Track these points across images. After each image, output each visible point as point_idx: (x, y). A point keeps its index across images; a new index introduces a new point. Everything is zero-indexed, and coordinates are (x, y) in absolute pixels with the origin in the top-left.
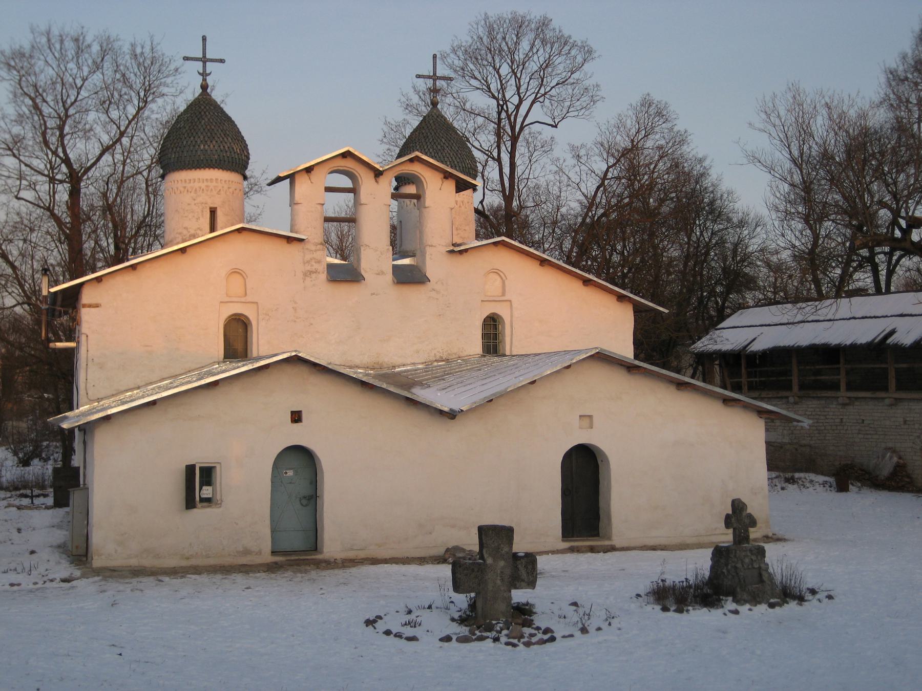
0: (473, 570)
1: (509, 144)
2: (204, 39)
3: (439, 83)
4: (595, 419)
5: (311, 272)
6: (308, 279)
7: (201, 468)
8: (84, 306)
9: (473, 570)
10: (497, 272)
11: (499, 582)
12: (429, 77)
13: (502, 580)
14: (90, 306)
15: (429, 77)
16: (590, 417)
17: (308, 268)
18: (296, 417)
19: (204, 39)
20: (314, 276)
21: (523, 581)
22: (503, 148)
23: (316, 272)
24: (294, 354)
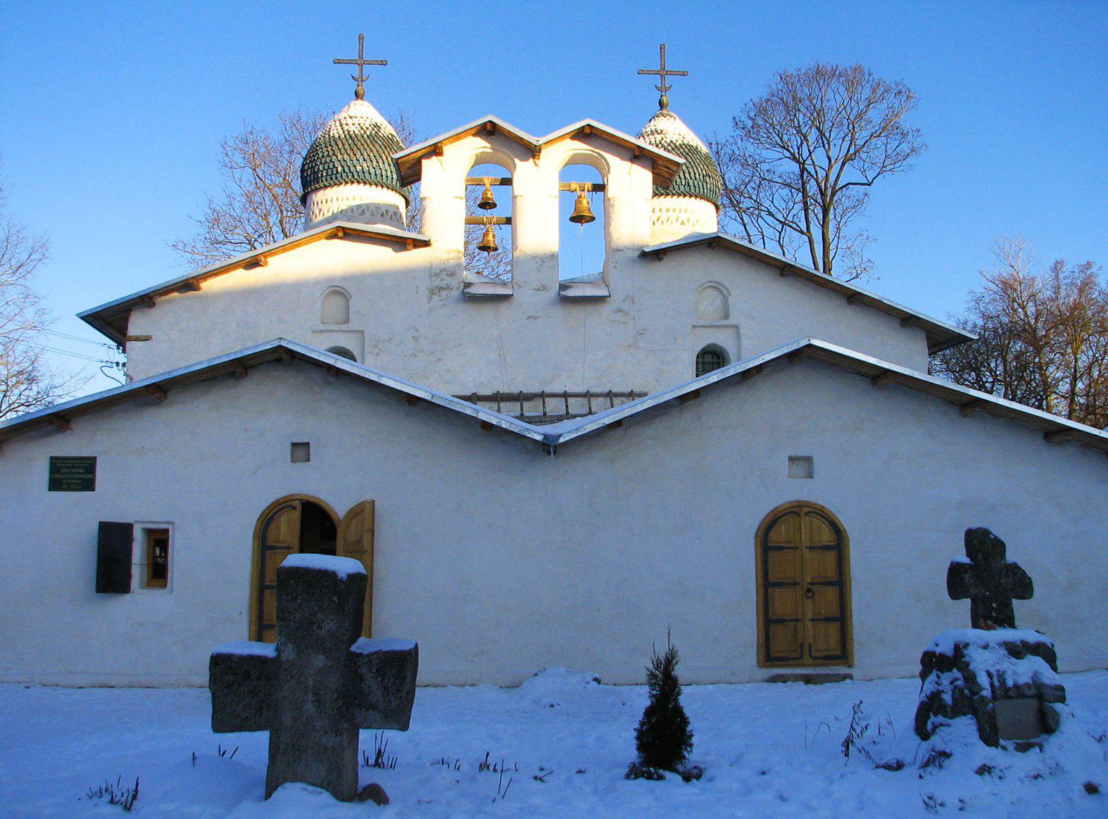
0: (247, 675)
1: (819, 210)
2: (361, 38)
3: (669, 80)
4: (816, 462)
5: (441, 289)
6: (436, 298)
7: (149, 532)
8: (131, 339)
9: (247, 675)
10: (717, 287)
11: (310, 708)
12: (656, 73)
13: (319, 702)
14: (137, 339)
15: (656, 73)
16: (808, 460)
17: (437, 283)
18: (301, 450)
19: (361, 38)
20: (444, 293)
21: (373, 707)
22: (811, 215)
23: (448, 288)
24: (276, 344)
